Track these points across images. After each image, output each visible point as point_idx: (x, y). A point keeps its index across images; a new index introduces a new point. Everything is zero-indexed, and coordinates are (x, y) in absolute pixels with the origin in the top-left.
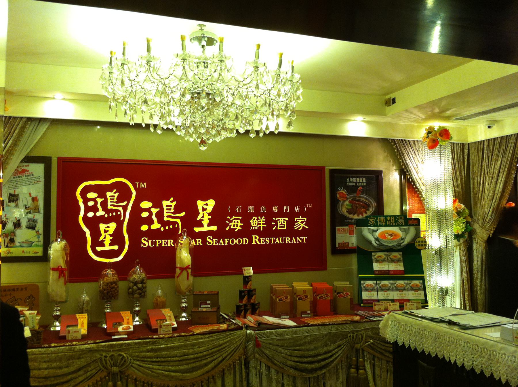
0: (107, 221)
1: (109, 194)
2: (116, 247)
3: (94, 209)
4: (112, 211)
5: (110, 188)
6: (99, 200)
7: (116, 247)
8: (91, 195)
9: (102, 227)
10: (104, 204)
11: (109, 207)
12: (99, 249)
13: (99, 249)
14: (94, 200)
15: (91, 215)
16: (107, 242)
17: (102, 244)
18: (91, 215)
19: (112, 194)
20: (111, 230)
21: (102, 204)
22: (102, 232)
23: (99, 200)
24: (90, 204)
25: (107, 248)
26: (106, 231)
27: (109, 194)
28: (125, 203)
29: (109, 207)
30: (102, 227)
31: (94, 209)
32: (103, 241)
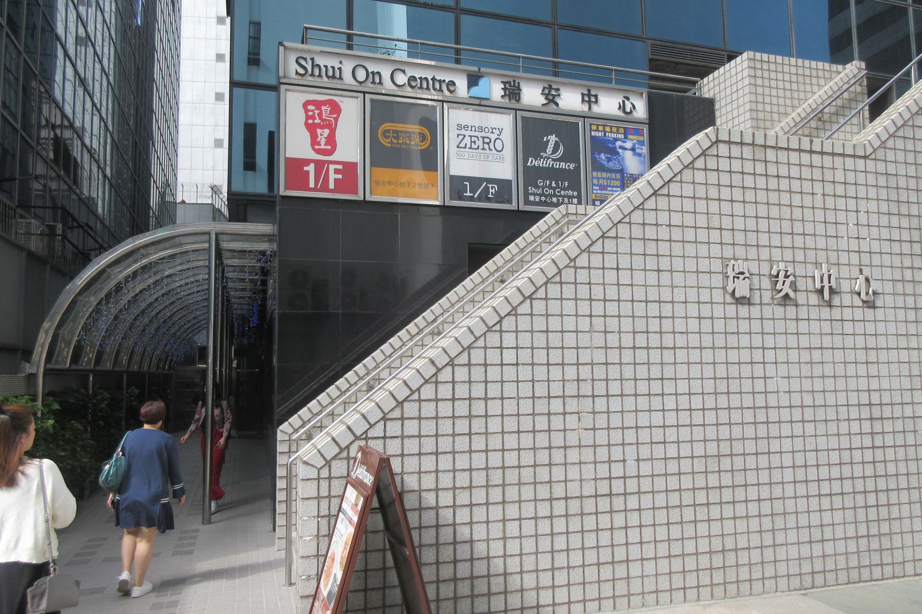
0: (322, 127)
1: (323, 108)
2: (329, 147)
3: (313, 118)
4: (326, 120)
5: (324, 103)
6: (317, 112)
7: (329, 147)
8: (311, 107)
9: (319, 131)
10: (320, 115)
11: (324, 117)
12: (317, 147)
13: (317, 147)
14: (313, 111)
15: (310, 121)
16: (323, 143)
17: (319, 144)
18: (310, 121)
19: (325, 108)
20: (326, 135)
21: (318, 114)
22: (319, 135)
23: (317, 112)
24: (311, 113)
25: (323, 147)
26: (321, 135)
27: (323, 108)
28: (335, 116)
29: (324, 117)
30: (319, 131)
31: (313, 118)
32: (319, 142)
